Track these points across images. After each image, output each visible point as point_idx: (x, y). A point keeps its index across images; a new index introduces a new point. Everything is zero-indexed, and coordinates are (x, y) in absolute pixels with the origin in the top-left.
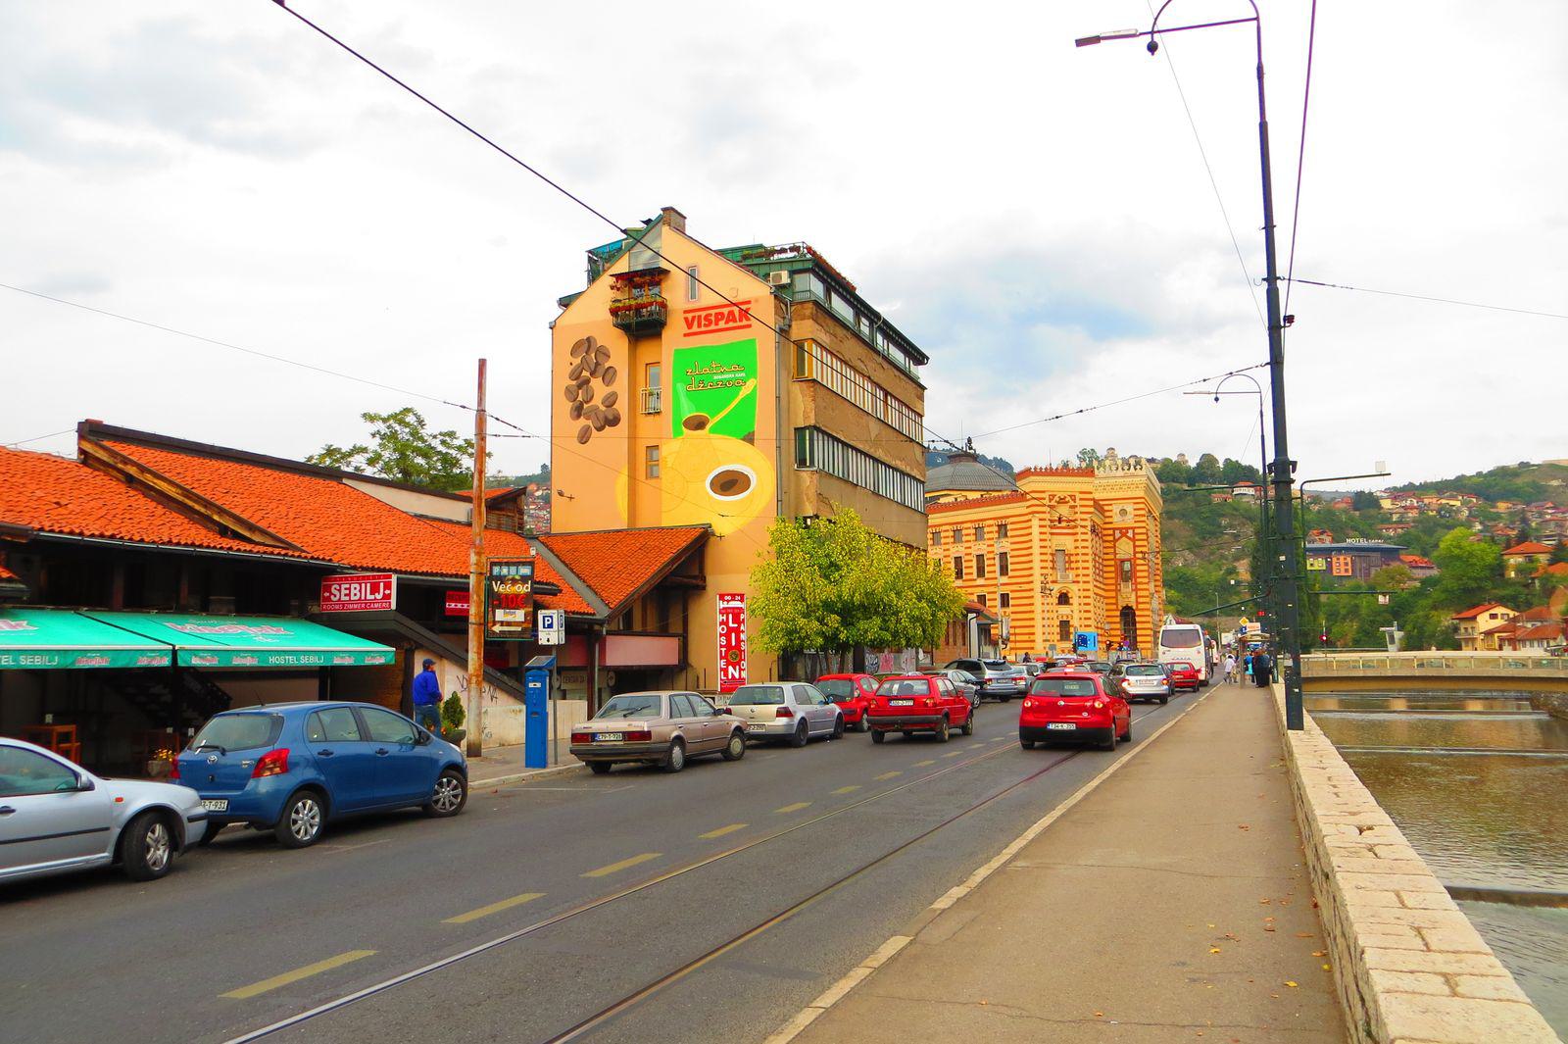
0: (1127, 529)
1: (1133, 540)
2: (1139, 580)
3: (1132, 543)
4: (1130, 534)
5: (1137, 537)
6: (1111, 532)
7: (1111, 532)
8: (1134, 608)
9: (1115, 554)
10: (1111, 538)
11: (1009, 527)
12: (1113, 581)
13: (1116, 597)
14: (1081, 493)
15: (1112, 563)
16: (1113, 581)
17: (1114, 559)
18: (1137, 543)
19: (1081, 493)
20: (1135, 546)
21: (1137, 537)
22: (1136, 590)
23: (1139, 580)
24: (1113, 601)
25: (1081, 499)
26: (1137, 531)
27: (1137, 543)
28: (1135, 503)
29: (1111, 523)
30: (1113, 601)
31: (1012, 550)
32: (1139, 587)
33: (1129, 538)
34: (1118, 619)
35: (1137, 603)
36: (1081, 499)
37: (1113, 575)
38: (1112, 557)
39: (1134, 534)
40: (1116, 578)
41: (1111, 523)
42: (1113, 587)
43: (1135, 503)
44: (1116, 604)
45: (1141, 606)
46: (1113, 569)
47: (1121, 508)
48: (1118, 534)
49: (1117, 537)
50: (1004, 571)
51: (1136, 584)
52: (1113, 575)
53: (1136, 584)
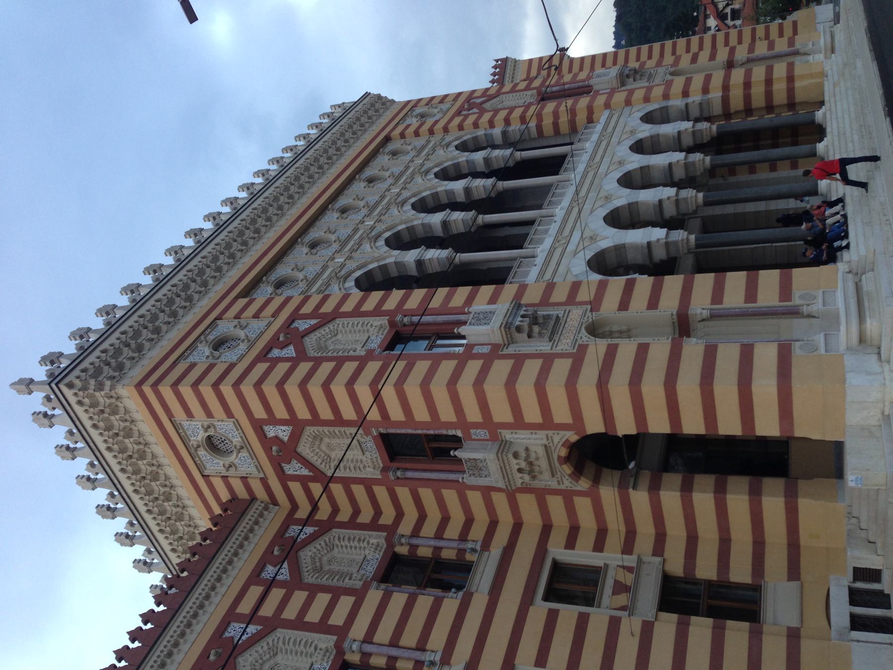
3: (309, 430)
6: (296, 488)
7: (296, 488)
8: (574, 438)
9: (368, 484)
15: (404, 493)
20: (316, 421)
26: (259, 413)
27: (303, 413)
29: (264, 481)
32: (473, 414)
33: (296, 437)
34: (640, 498)
35: (548, 423)
38: (381, 493)
39: (273, 421)
41: (264, 481)
45: (561, 413)
46: (427, 495)
48: (293, 468)
49: (305, 472)
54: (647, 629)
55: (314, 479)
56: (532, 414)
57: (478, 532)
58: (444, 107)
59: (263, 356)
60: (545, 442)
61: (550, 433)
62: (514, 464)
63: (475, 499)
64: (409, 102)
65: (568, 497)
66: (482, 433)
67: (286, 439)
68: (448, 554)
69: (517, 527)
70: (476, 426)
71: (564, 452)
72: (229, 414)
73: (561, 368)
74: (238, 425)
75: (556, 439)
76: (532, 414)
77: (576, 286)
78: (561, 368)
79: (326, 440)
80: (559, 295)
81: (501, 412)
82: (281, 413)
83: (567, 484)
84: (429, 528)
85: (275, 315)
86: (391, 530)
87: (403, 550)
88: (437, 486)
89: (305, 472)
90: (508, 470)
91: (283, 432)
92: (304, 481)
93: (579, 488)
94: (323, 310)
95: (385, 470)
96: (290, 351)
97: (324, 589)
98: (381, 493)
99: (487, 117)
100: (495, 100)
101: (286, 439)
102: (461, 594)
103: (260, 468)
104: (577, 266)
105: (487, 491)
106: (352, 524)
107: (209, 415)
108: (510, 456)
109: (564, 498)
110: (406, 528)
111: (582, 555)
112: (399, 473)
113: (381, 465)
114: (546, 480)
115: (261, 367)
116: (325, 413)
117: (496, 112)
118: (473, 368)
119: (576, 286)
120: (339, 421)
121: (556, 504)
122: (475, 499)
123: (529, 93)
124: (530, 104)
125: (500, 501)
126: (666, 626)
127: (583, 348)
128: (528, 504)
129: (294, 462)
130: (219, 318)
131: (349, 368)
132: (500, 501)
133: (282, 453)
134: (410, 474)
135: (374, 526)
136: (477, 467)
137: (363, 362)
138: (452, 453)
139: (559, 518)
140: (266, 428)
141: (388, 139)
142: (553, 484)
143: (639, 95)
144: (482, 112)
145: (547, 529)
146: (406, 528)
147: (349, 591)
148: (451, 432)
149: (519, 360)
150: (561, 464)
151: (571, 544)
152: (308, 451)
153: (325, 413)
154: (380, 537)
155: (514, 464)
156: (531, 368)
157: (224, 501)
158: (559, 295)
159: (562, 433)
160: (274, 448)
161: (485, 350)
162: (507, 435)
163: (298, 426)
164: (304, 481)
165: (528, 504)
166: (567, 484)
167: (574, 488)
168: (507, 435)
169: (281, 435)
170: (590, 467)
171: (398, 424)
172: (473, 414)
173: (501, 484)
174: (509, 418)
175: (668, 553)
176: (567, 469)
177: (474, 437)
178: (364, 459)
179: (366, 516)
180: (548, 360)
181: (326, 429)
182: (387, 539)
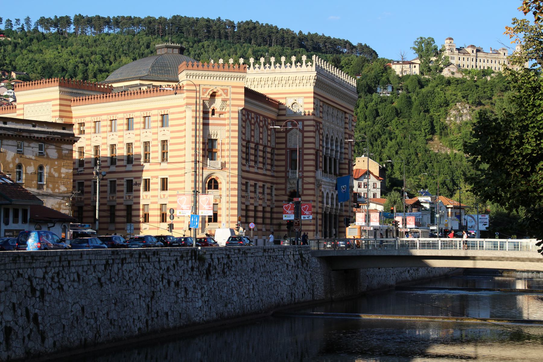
0: (298, 121)
1: (302, 131)
2: (306, 168)
3: (301, 134)
4: (300, 126)
5: (306, 129)
9: (286, 143)
11: (170, 117)
12: (283, 169)
13: (285, 183)
14: (233, 87)
15: (283, 152)
16: (283, 169)
17: (286, 149)
18: (306, 134)
19: (233, 87)
20: (304, 137)
21: (306, 129)
22: (302, 177)
23: (306, 168)
24: (283, 186)
25: (233, 93)
26: (306, 123)
27: (306, 134)
28: (305, 97)
29: (284, 115)
30: (283, 186)
31: (172, 138)
32: (305, 174)
36: (233, 93)
37: (283, 163)
38: (283, 146)
39: (304, 126)
40: (286, 166)
41: (284, 115)
42: (283, 174)
43: (305, 97)
44: (285, 189)
45: (306, 192)
46: (283, 157)
50: (164, 157)
51: (303, 171)
52: (283, 163)
53: (303, 171)
81: (306, 180)
83: (288, 190)
88: (286, 160)
95: (290, 149)
98: (283, 146)
111: (274, 192)
114: (289, 186)
116: (306, 140)
141: (345, 113)
145: (277, 184)
151: (276, 189)
166: (288, 190)
172: (305, 174)
176: (292, 190)
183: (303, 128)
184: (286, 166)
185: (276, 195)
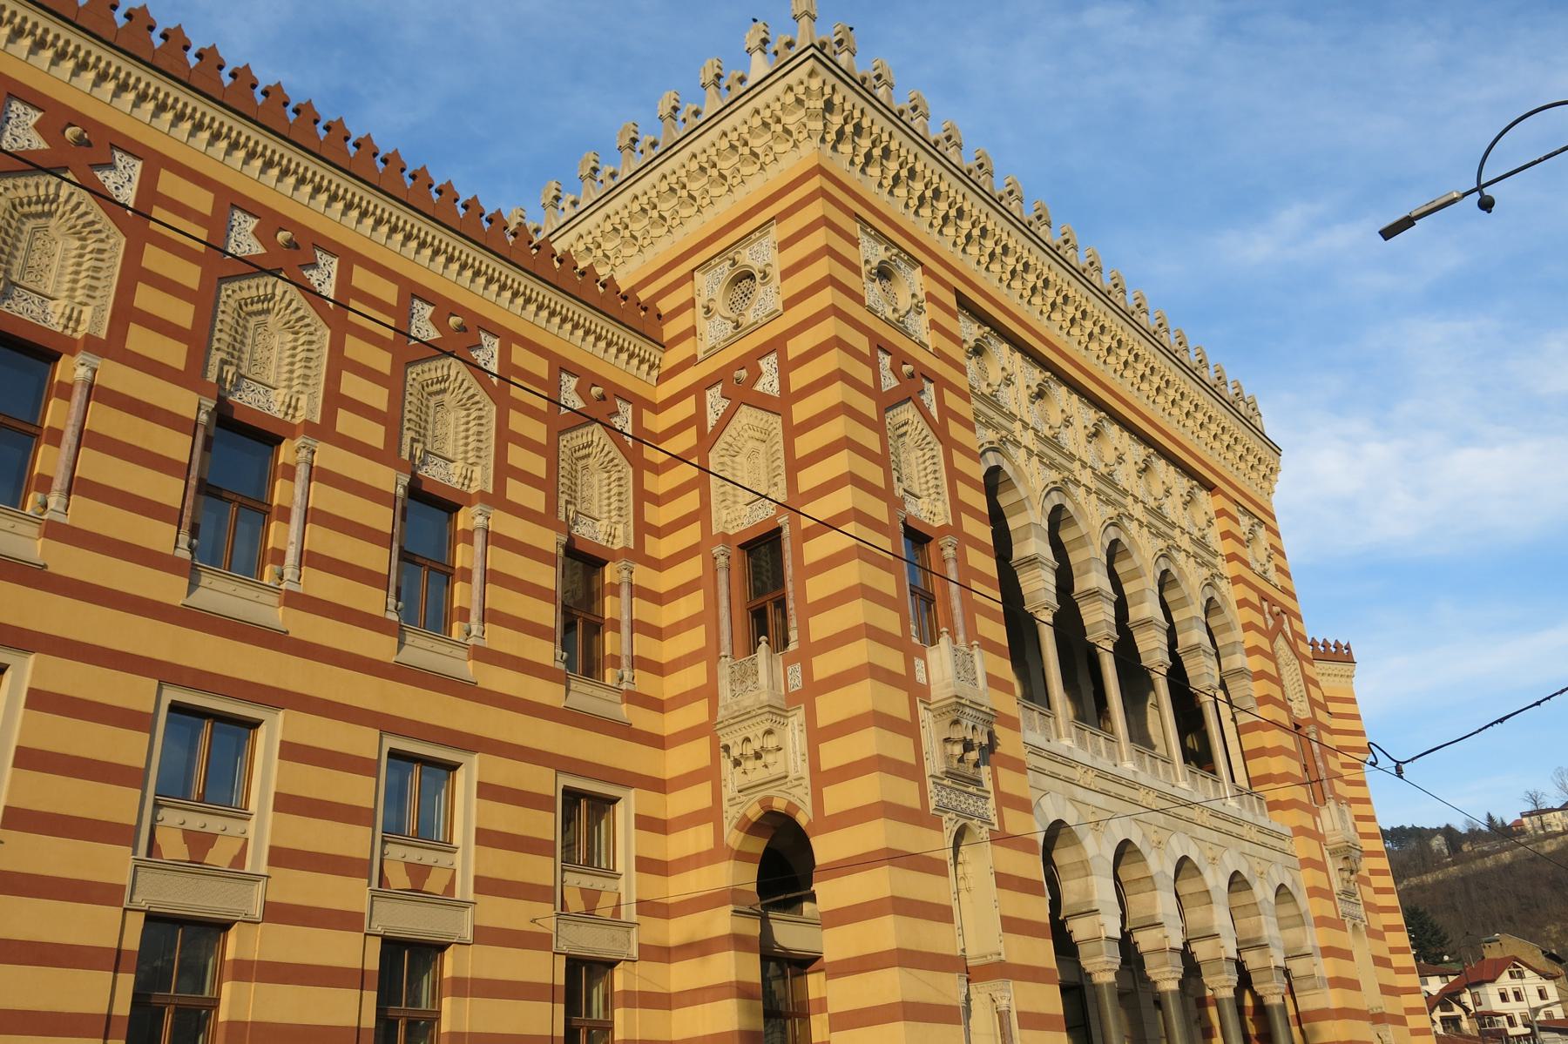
3: (776, 422)
6: (687, 408)
7: (687, 408)
8: (803, 819)
9: (702, 514)
10: (687, 440)
15: (692, 569)
20: (792, 432)
22: (813, 689)
23: (821, 626)
26: (795, 347)
27: (802, 411)
29: (692, 361)
32: (824, 666)
33: (763, 403)
35: (821, 779)
41: (692, 361)
44: (712, 815)
45: (838, 798)
46: (692, 604)
47: (724, 270)
48: (715, 402)
49: (712, 420)
54: (539, 941)
55: (702, 434)
56: (834, 754)
57: (646, 683)
58: (1273, 575)
59: (881, 345)
60: (792, 775)
61: (807, 782)
62: (755, 730)
63: (694, 677)
64: (1273, 518)
65: (712, 815)
66: (796, 681)
67: (759, 388)
68: (610, 643)
69: (658, 742)
70: (807, 672)
71: (779, 805)
72: (789, 303)
73: (905, 793)
74: (774, 316)
75: (799, 792)
76: (834, 754)
77: (1025, 806)
78: (905, 793)
79: (762, 447)
80: (1011, 782)
81: (831, 708)
82: (799, 378)
83: (731, 814)
84: (645, 611)
85: (939, 354)
86: (637, 554)
87: (610, 573)
88: (707, 617)
89: (712, 420)
90: (745, 724)
91: (768, 383)
92: (698, 418)
93: (727, 829)
94: (952, 424)
95: (725, 538)
96: (889, 382)
97: (553, 467)
99: (1264, 643)
100: (1289, 653)
101: (759, 388)
102: (562, 666)
103: (712, 352)
104: (1052, 808)
105: (709, 692)
106: (643, 496)
107: (786, 274)
108: (767, 726)
109: (709, 810)
110: (643, 576)
112: (722, 560)
113: (731, 533)
114: (732, 779)
115: (862, 344)
116: (806, 444)
117: (1272, 657)
118: (893, 660)
119: (1025, 806)
120: (795, 466)
121: (697, 797)
122: (694, 677)
123: (1306, 706)
124: (1289, 710)
125: (696, 713)
126: (547, 969)
127: (936, 824)
128: (693, 755)
129: (726, 403)
130: (927, 271)
131: (875, 474)
132: (696, 713)
133: (738, 386)
134: (722, 576)
135: (643, 528)
136: (743, 677)
137: (885, 494)
138: (763, 638)
139: (677, 804)
140: (773, 358)
142: (728, 792)
143: (1318, 879)
144: (1272, 635)
146: (643, 576)
147: (552, 503)
148: (793, 635)
149: (910, 729)
150: (760, 802)
152: (744, 421)
153: (806, 444)
154: (626, 538)
155: (755, 730)
156: (901, 749)
157: (658, 304)
158: (1011, 782)
159: (808, 800)
160: (744, 373)
161: (921, 677)
162: (797, 718)
163: (778, 406)
164: (698, 418)
165: (693, 755)
166: (731, 814)
167: (726, 822)
168: (797, 718)
169: (763, 380)
170: (758, 846)
171: (798, 555)
172: (824, 666)
173: (722, 713)
174: (823, 720)
175: (644, 967)
176: (754, 812)
177: (790, 669)
178: (739, 506)
179: (658, 516)
180: (913, 772)
181: (780, 446)
182: (625, 549)
183: (784, 382)
184: (708, 655)
185: (645, 865)
